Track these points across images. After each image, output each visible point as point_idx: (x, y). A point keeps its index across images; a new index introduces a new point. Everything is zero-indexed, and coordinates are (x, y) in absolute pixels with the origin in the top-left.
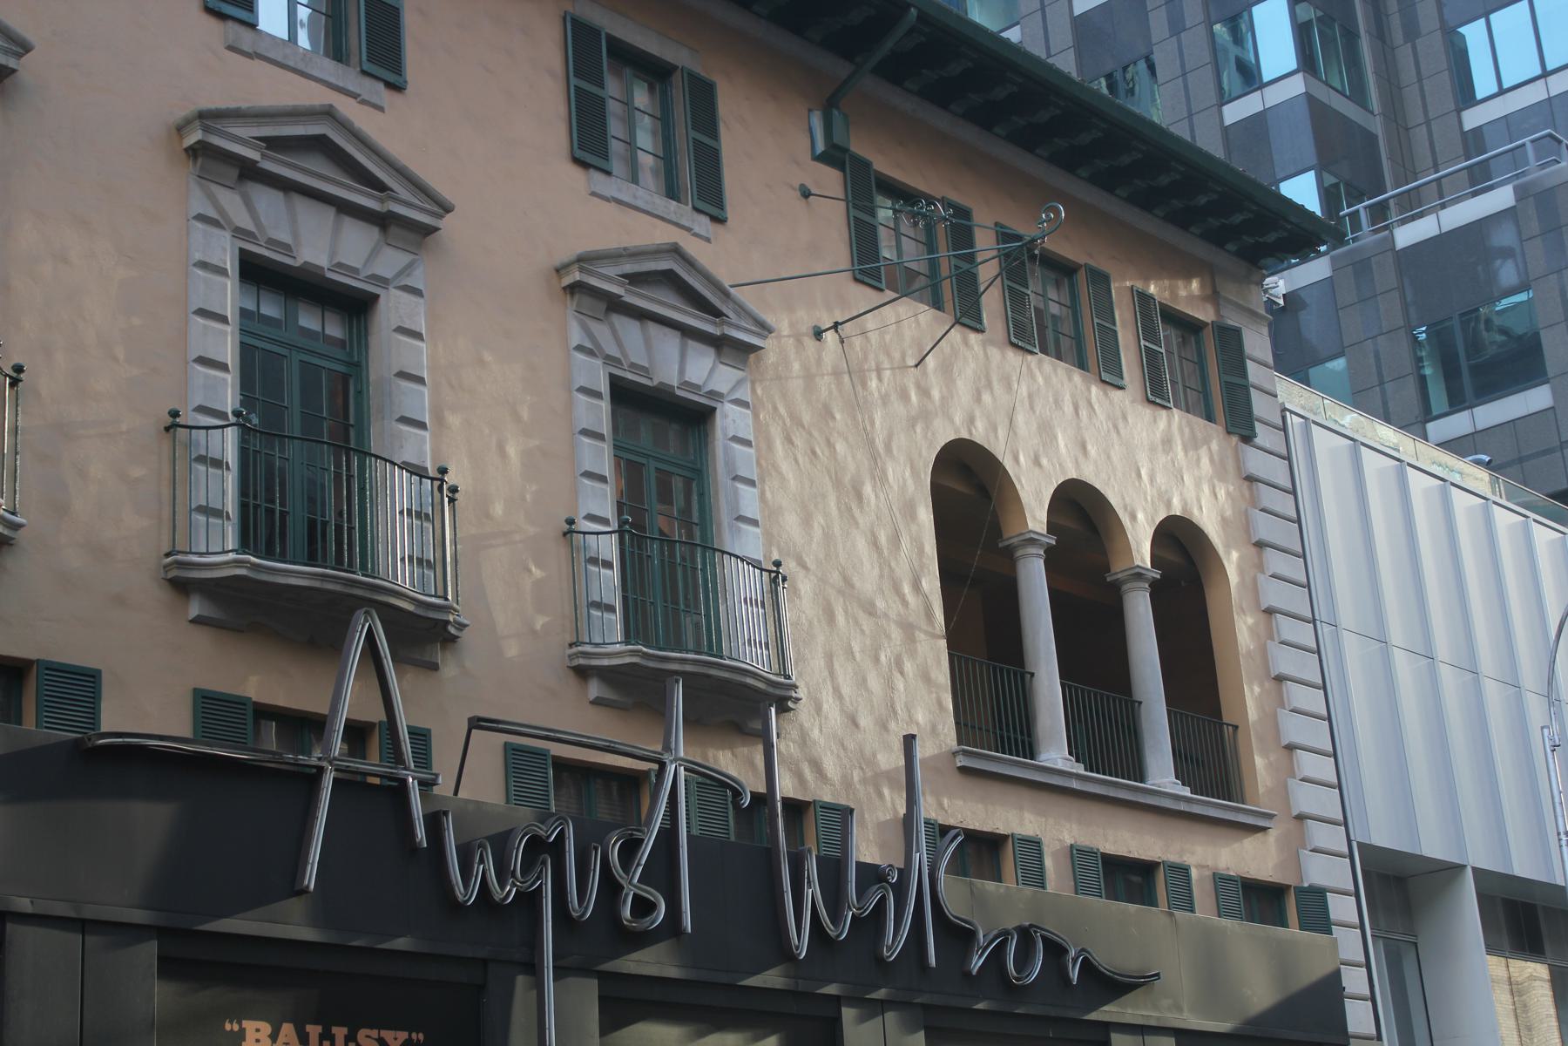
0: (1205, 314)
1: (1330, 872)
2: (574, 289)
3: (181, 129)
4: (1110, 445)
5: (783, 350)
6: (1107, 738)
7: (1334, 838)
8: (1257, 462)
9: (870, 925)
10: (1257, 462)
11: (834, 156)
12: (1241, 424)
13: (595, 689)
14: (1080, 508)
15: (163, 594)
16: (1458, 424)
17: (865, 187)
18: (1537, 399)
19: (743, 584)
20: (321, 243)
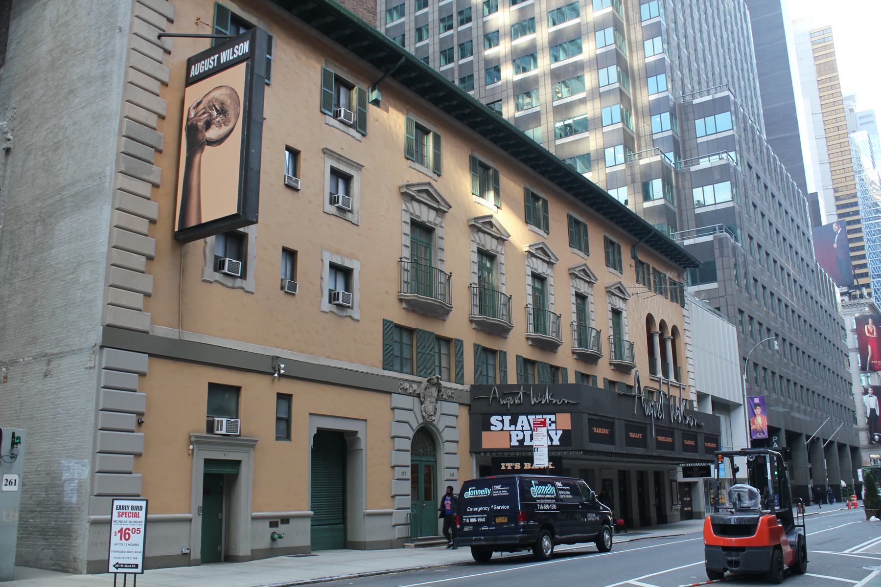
0: (677, 280)
1: (694, 397)
2: (608, 292)
3: (569, 270)
4: (662, 309)
5: (631, 300)
6: (665, 373)
7: (693, 390)
8: (685, 312)
9: (678, 417)
10: (685, 312)
11: (634, 257)
12: (683, 305)
13: (613, 367)
14: (663, 324)
15: (571, 354)
16: (696, 288)
17: (639, 264)
18: (714, 285)
19: (626, 345)
20: (584, 288)
